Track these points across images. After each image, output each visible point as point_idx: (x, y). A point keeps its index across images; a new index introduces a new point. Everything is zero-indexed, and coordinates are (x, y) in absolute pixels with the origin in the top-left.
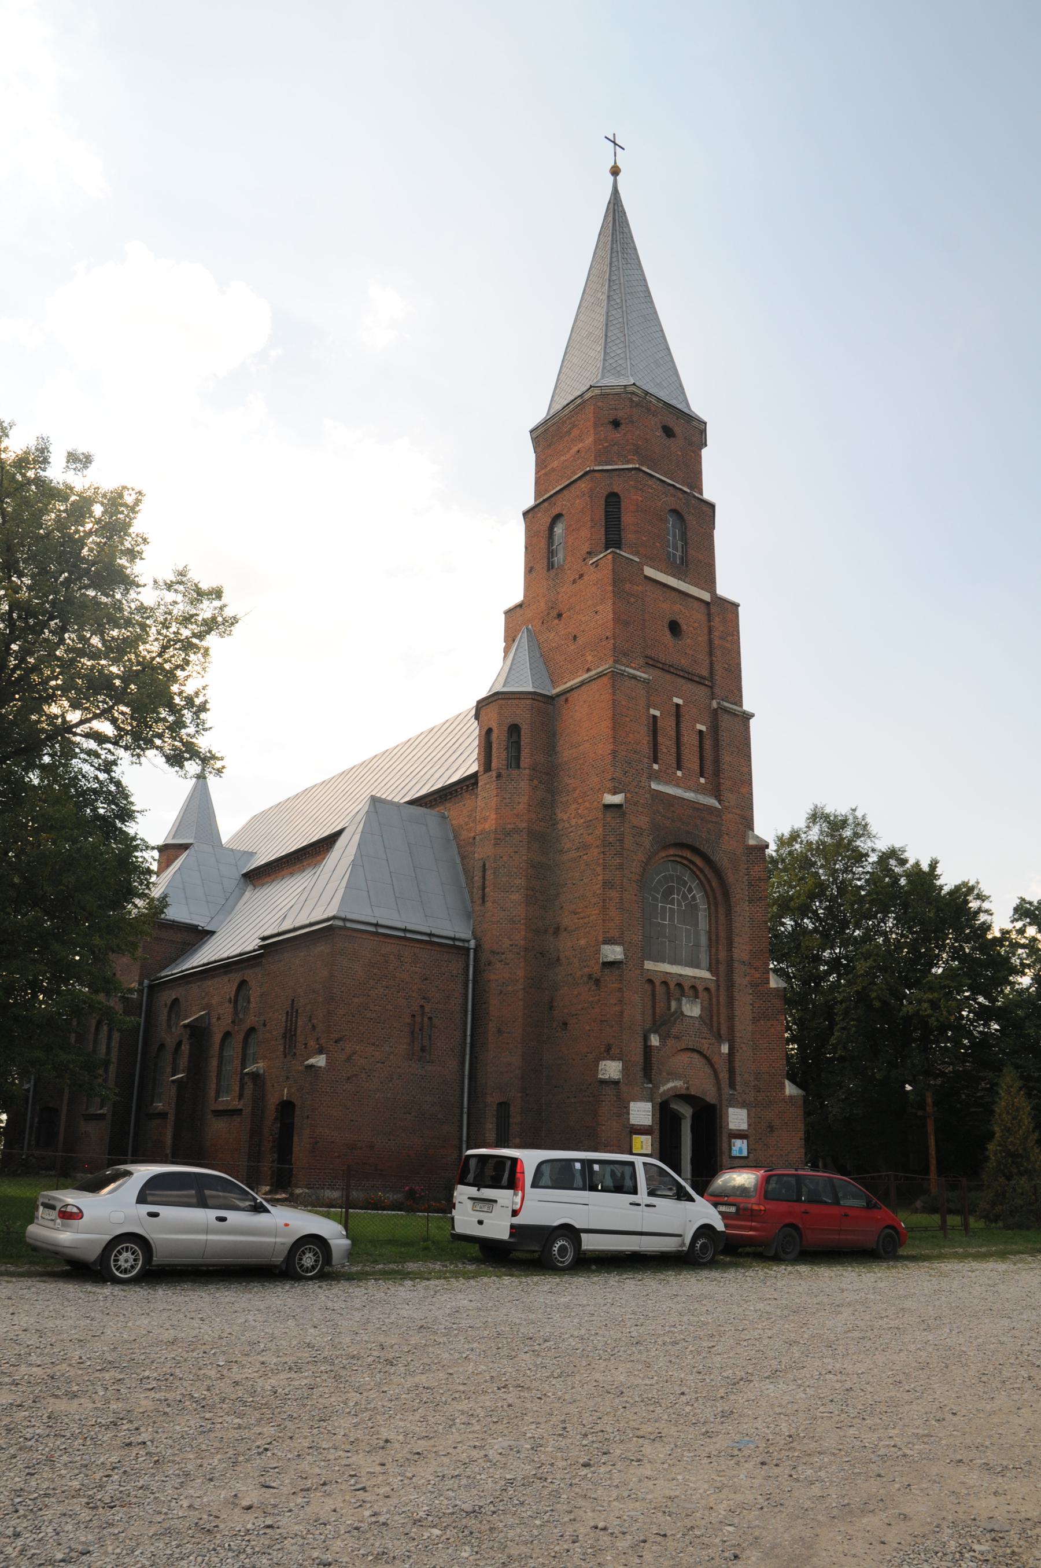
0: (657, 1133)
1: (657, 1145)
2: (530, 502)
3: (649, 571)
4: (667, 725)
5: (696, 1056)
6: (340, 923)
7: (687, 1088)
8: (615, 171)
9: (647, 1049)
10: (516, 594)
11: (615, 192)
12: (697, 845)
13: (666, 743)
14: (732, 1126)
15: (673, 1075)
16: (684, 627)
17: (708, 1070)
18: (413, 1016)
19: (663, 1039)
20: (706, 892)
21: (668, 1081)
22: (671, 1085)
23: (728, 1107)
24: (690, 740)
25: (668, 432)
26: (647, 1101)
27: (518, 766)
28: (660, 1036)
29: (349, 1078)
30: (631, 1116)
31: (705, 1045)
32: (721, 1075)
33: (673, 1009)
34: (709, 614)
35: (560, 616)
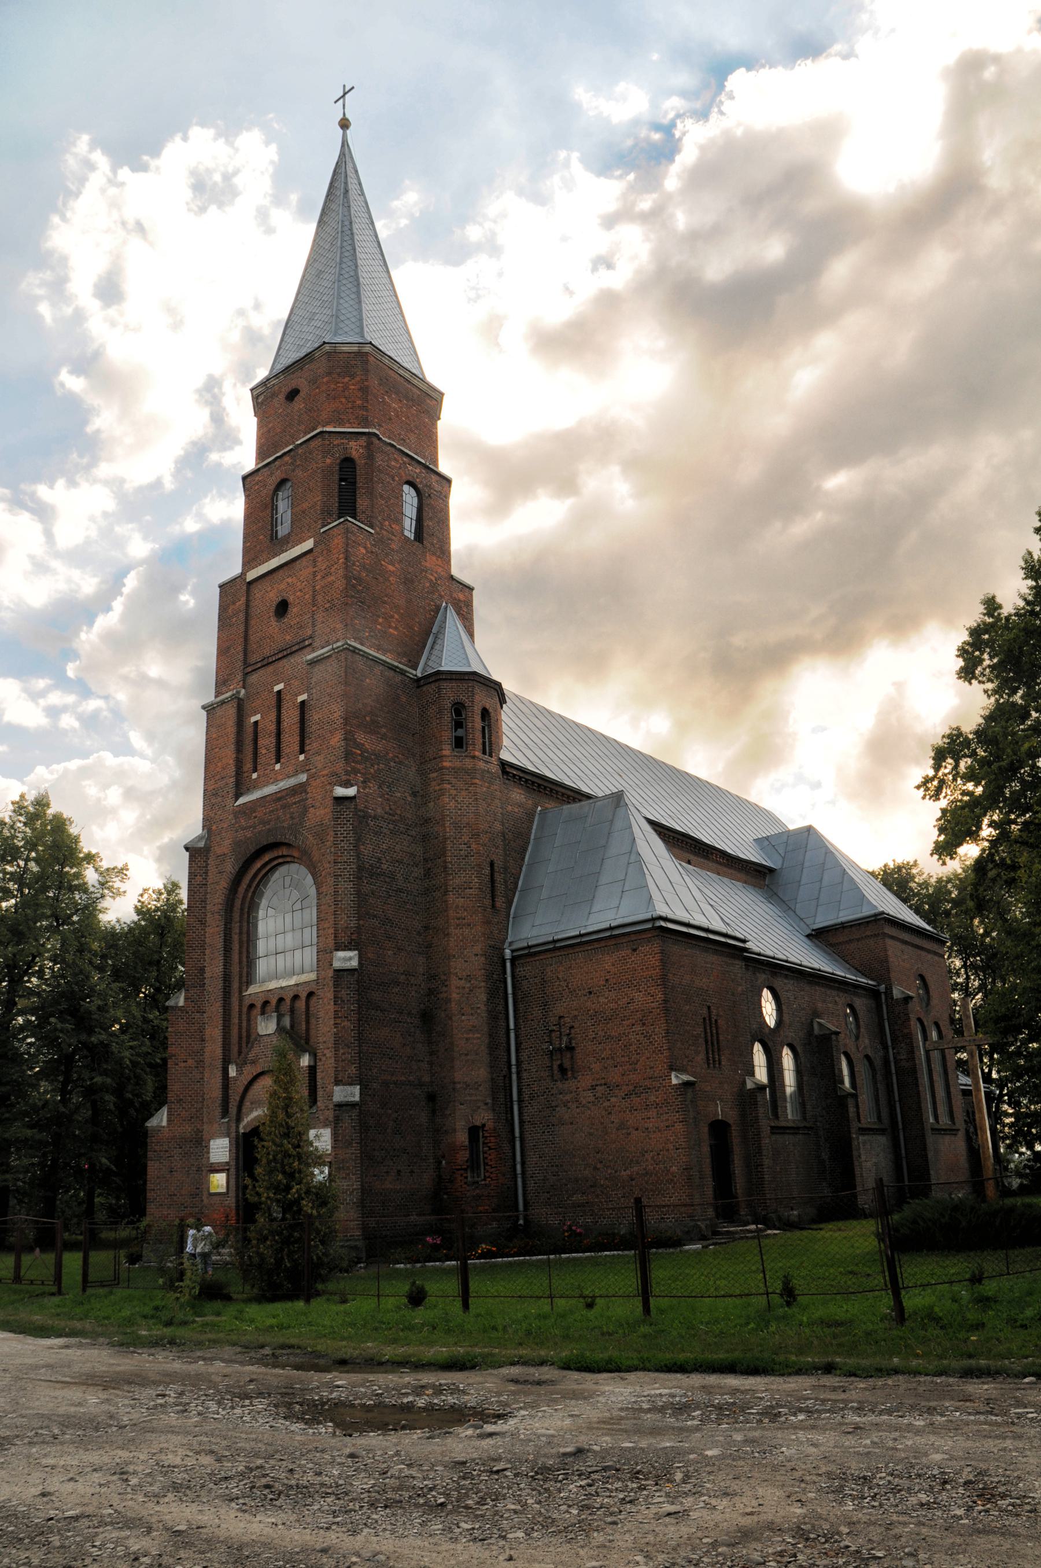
0: (233, 1171)
1: (233, 1182)
8: (344, 124)
11: (345, 143)
12: (279, 838)
21: (251, 1111)
22: (255, 1114)
26: (225, 1137)
28: (237, 1065)
30: (211, 1154)
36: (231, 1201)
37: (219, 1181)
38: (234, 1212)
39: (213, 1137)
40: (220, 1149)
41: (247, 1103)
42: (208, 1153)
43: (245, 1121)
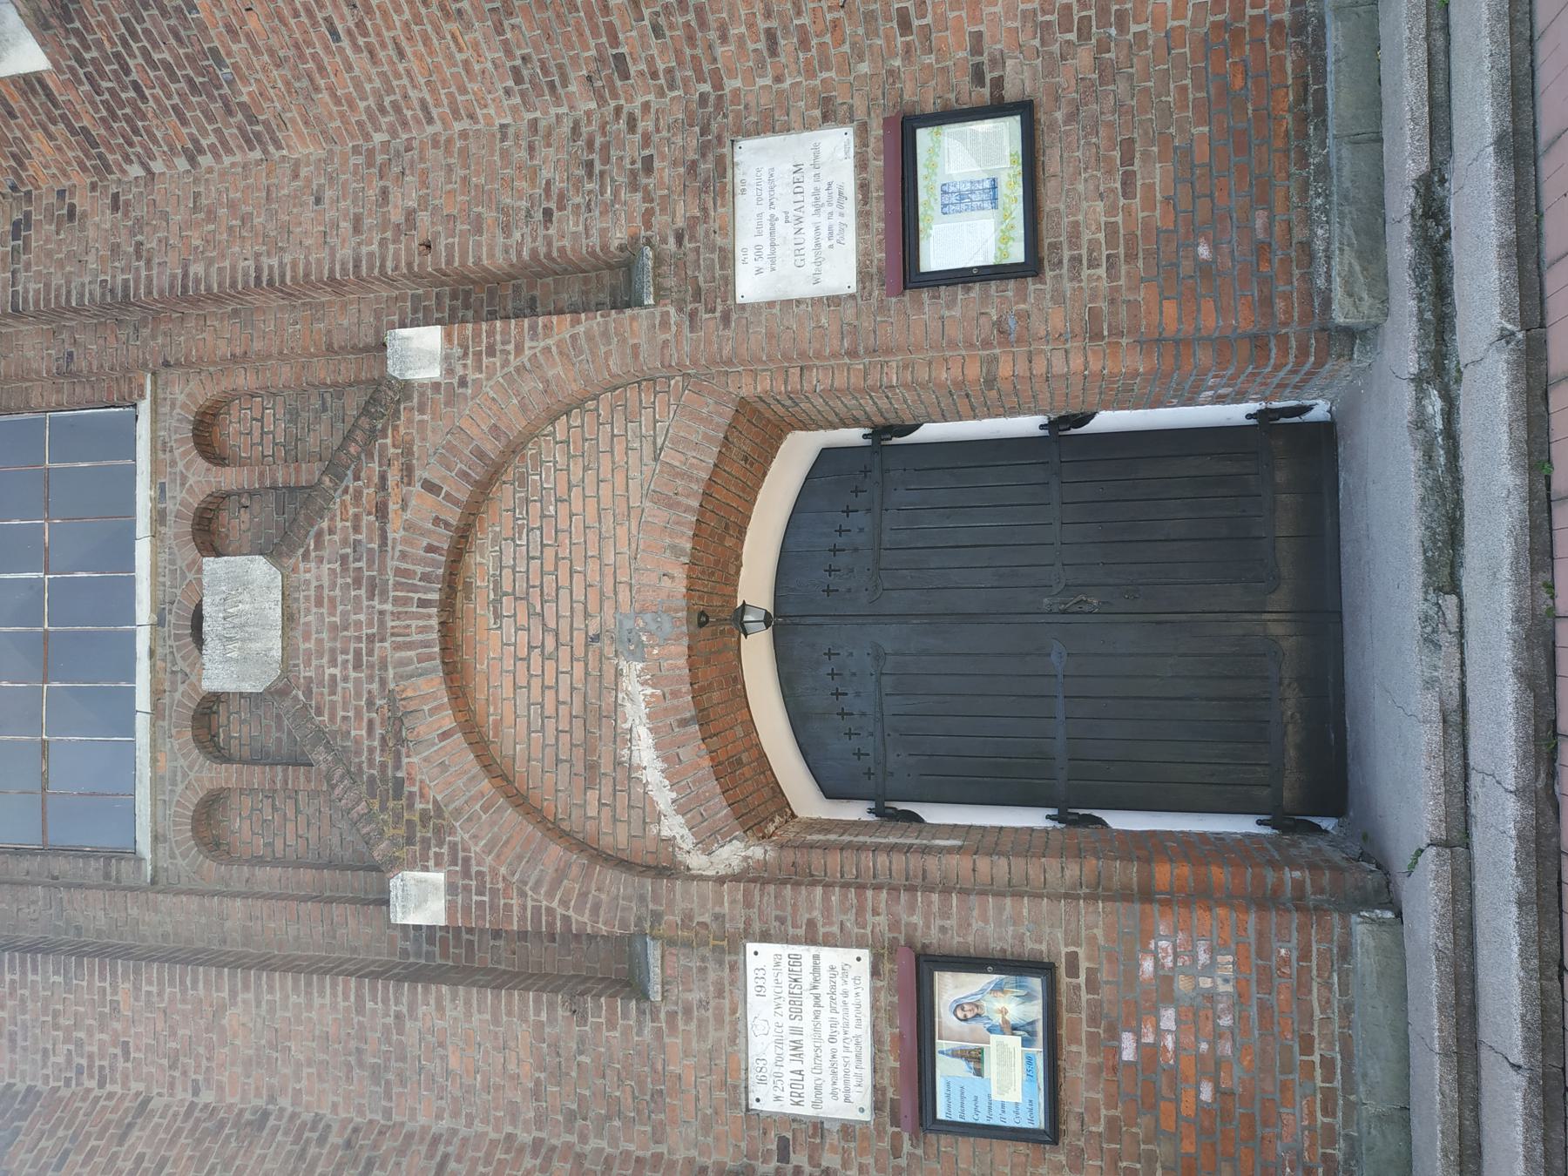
19: (426, 835)
21: (628, 772)
22: (644, 751)
26: (737, 970)
31: (418, 516)
39: (731, 1080)
41: (589, 809)
42: (818, 1127)
43: (674, 827)
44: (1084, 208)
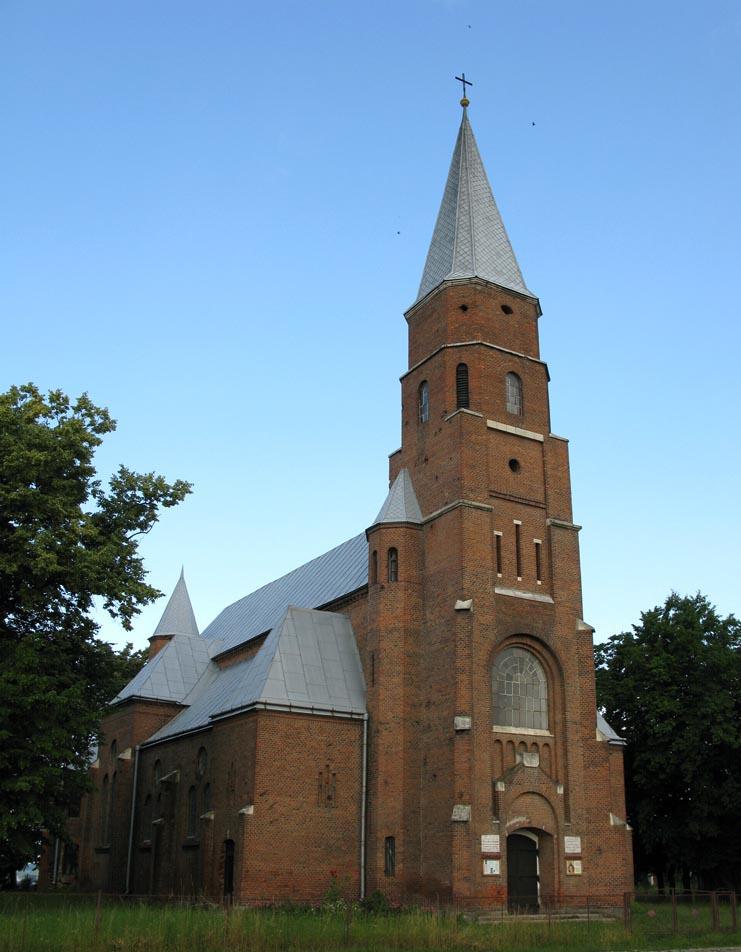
0: (504, 859)
1: (505, 868)
2: (405, 370)
3: (491, 424)
4: (509, 544)
5: (536, 797)
6: (262, 707)
7: (530, 822)
8: (465, 104)
9: (495, 794)
10: (396, 444)
11: (465, 118)
12: (534, 634)
13: (508, 556)
14: (567, 850)
15: (518, 813)
16: (522, 464)
17: (546, 807)
18: (321, 773)
20: (544, 668)
22: (516, 820)
23: (564, 835)
24: (528, 552)
25: (507, 310)
27: (396, 580)
28: (505, 783)
29: (271, 822)
31: (543, 789)
32: (558, 812)
33: (517, 762)
34: (543, 452)
35: (426, 460)
36: (504, 883)
37: (493, 867)
38: (506, 889)
39: (486, 833)
40: (491, 843)
44: (573, 881)
